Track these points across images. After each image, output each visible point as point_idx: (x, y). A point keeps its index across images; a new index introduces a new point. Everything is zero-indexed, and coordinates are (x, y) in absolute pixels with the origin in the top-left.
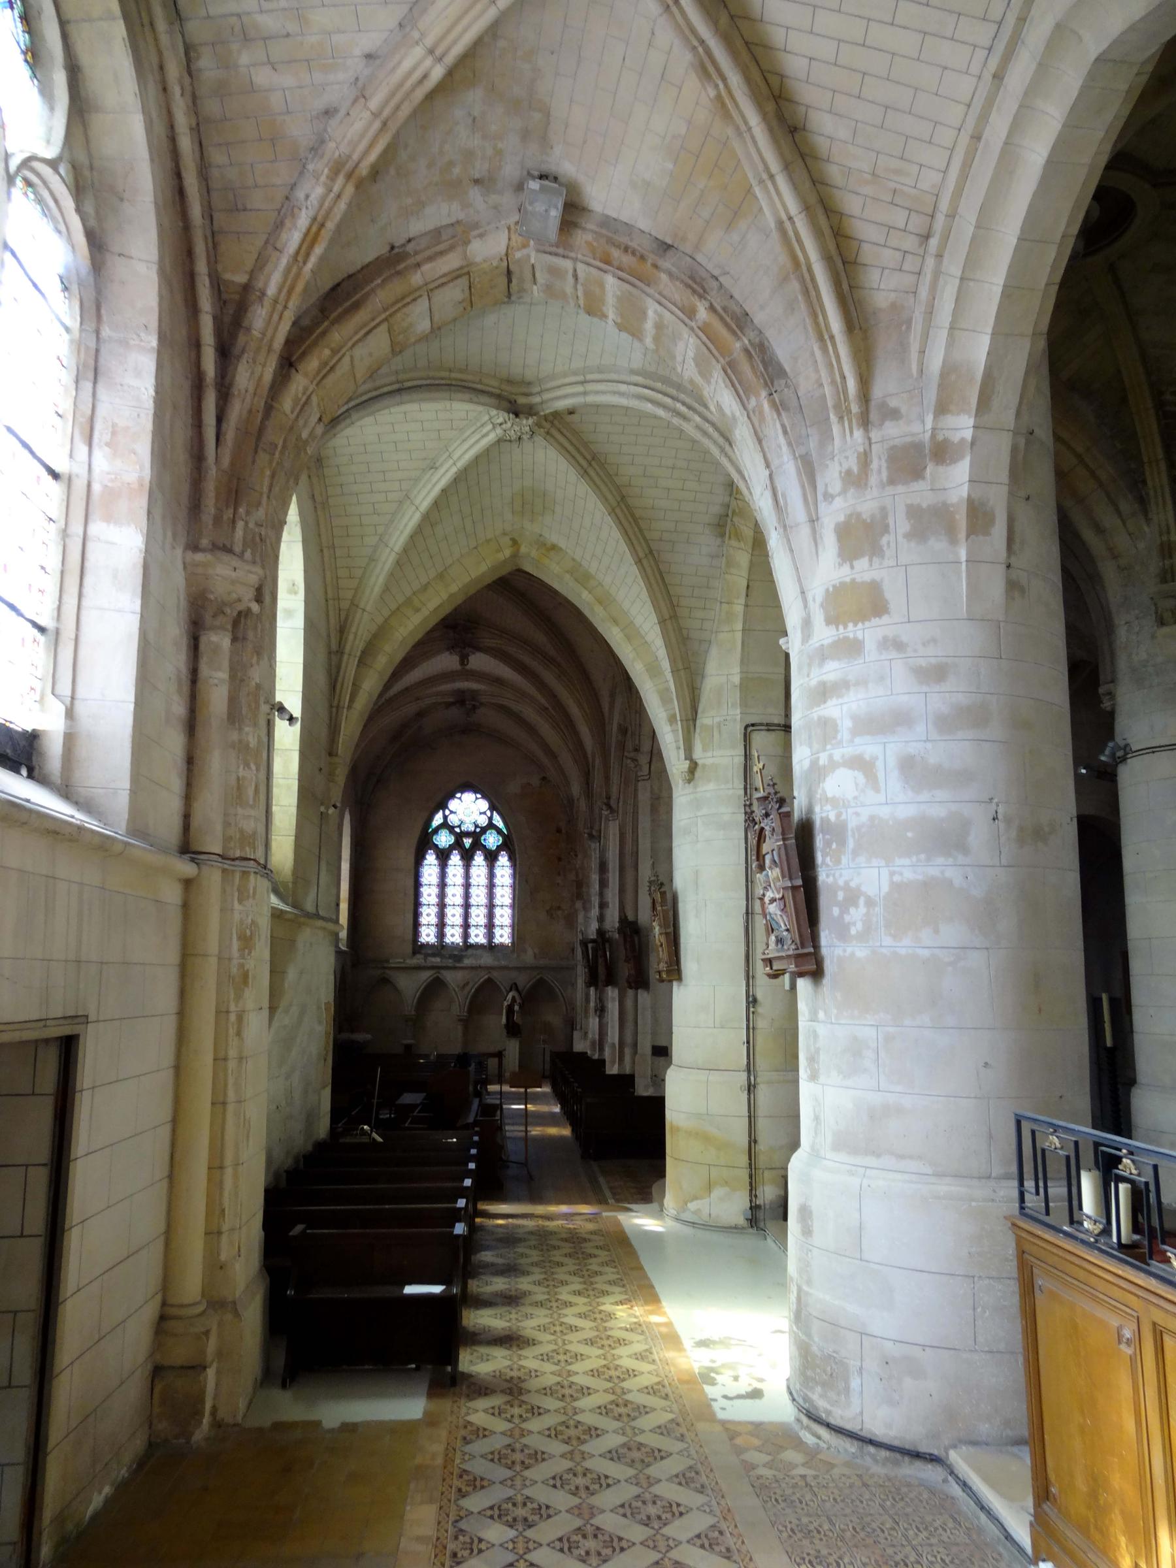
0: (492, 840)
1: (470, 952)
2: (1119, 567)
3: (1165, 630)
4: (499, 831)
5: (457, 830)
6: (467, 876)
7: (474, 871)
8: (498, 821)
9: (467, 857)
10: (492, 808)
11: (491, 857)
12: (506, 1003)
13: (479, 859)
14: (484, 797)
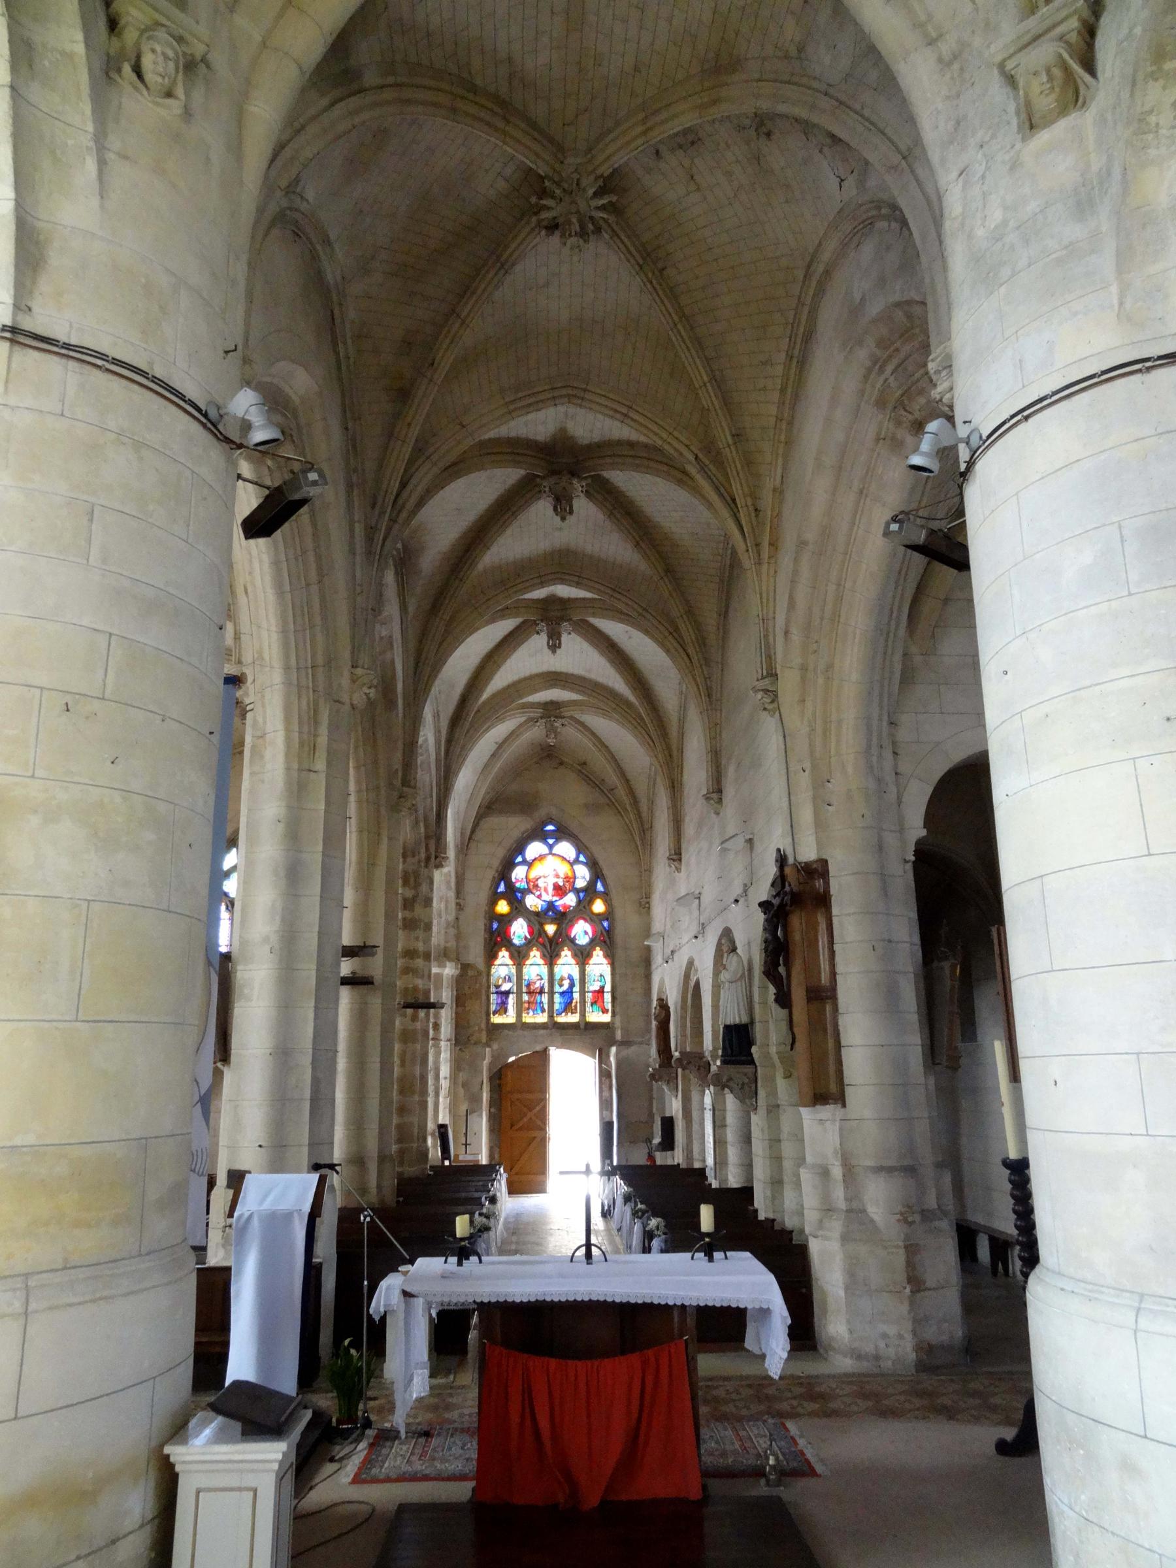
2: (940, 60)
3: (1044, 137)
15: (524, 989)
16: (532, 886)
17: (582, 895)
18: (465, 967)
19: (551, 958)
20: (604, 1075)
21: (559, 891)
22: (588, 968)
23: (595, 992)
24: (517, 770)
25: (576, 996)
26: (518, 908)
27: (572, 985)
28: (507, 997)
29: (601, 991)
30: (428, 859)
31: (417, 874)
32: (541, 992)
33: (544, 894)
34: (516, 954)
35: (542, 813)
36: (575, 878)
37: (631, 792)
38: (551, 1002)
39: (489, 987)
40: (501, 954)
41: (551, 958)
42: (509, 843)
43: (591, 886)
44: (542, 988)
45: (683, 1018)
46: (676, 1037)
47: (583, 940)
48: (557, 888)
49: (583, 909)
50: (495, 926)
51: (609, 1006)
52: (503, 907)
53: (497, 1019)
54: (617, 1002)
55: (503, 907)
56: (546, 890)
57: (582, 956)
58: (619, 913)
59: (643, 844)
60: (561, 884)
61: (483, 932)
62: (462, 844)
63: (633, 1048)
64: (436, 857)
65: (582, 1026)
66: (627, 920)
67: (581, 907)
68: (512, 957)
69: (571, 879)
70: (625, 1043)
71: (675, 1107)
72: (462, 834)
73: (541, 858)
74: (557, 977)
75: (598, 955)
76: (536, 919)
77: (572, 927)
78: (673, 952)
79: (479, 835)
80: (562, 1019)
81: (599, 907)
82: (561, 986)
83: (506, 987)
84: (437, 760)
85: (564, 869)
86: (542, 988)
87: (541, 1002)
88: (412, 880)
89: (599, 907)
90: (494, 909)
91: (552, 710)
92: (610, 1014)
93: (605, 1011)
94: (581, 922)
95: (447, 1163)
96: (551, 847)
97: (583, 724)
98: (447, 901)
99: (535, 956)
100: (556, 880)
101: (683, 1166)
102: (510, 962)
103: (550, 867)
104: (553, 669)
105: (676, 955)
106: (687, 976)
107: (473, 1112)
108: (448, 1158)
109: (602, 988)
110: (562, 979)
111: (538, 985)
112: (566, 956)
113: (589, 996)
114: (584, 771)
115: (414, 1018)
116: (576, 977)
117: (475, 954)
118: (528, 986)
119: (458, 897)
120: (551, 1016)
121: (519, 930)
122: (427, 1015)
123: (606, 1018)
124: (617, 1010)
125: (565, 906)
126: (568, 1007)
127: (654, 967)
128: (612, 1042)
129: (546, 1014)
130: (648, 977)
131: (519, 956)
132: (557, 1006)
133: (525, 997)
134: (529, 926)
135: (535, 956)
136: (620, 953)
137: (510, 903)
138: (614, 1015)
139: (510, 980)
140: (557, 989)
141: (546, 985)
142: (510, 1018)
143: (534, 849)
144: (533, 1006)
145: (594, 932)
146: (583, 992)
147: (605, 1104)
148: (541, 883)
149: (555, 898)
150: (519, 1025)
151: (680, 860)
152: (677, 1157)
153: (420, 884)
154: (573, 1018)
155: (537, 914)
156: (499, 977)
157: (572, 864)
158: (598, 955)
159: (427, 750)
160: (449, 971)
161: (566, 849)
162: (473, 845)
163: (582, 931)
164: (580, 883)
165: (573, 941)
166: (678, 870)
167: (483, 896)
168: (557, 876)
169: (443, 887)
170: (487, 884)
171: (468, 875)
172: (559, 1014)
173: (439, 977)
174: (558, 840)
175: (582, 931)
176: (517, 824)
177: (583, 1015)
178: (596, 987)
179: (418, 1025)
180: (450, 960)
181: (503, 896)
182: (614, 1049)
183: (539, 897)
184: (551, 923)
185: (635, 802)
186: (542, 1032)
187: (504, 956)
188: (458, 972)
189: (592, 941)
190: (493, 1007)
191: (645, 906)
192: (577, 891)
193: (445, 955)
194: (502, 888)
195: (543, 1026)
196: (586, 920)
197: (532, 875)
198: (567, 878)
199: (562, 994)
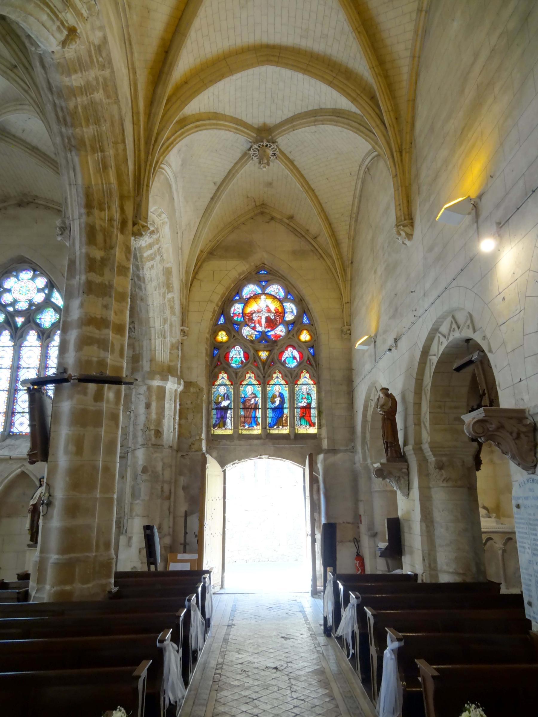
0: (48, 318)
1: (8, 441)
4: (56, 309)
5: (11, 309)
6: (17, 357)
7: (24, 352)
8: (58, 299)
9: (18, 336)
10: (51, 285)
11: (45, 336)
12: (32, 502)
13: (32, 337)
14: (44, 274)
15: (241, 406)
16: (248, 319)
17: (290, 327)
18: (188, 385)
19: (264, 381)
20: (313, 480)
21: (271, 323)
22: (297, 388)
23: (302, 408)
24: (234, 225)
25: (286, 411)
26: (235, 336)
27: (282, 402)
28: (226, 413)
29: (308, 407)
30: (124, 223)
31: (107, 234)
32: (256, 408)
33: (257, 325)
34: (234, 375)
35: (257, 258)
36: (284, 312)
37: (333, 234)
38: (264, 417)
39: (209, 403)
40: (220, 376)
41: (264, 381)
42: (228, 282)
43: (299, 317)
44: (256, 404)
45: (418, 405)
46: (406, 429)
47: (292, 364)
48: (268, 319)
49: (291, 340)
50: (216, 352)
51: (315, 420)
52: (222, 337)
53: (218, 432)
54: (324, 415)
55: (222, 337)
56: (260, 323)
57: (292, 378)
58: (323, 339)
59: (344, 281)
60: (273, 318)
61: (204, 355)
62: (187, 281)
63: (340, 456)
64: (134, 224)
65: (292, 437)
66: (331, 345)
67: (290, 336)
68: (229, 378)
69: (281, 314)
70: (332, 451)
71: (408, 506)
72: (187, 272)
73: (256, 297)
74: (270, 395)
75: (305, 378)
76: (251, 347)
77: (282, 353)
78: (396, 340)
79: (200, 276)
80: (274, 431)
81: (305, 336)
82: (273, 402)
83: (225, 403)
84: (135, 113)
85: (273, 306)
86: (256, 404)
87: (255, 417)
88: (100, 238)
89: (305, 336)
90: (215, 338)
91: (263, 138)
92: (316, 427)
93: (312, 424)
94: (290, 349)
95: (153, 568)
96: (263, 288)
97: (291, 162)
98: (171, 325)
99: (251, 378)
100: (267, 315)
101: (424, 578)
102: (228, 383)
103: (262, 304)
104: (265, 40)
105: (399, 343)
106: (425, 352)
107: (192, 513)
108: (154, 563)
109: (309, 404)
110: (274, 397)
111: (253, 401)
112: (277, 378)
113: (298, 412)
114: (291, 223)
115: (98, 397)
116: (286, 394)
117: (198, 374)
118: (244, 402)
119: (182, 325)
120: (264, 428)
121: (237, 355)
122: (118, 394)
123: (313, 430)
124: (324, 421)
125: (276, 336)
126: (278, 421)
127: (357, 380)
128: (319, 450)
129: (259, 427)
130: (350, 393)
131: (236, 379)
132: (269, 420)
133: (242, 413)
134: (245, 353)
135: (251, 378)
136: (325, 375)
137: (228, 333)
138: (320, 427)
139: (228, 398)
140: (269, 405)
141: (260, 402)
142: (228, 429)
143: (249, 290)
144: (249, 420)
145: (301, 357)
146: (292, 408)
147: (314, 507)
148: (255, 317)
149: (267, 330)
150: (236, 436)
151: (412, 225)
152: (412, 564)
153: (112, 248)
154: (285, 431)
155: (252, 342)
156: (219, 395)
157: (281, 301)
158: (305, 378)
159: (110, 62)
160: (173, 386)
161: (275, 289)
162: (196, 283)
163: (291, 357)
164: (289, 317)
165: (284, 364)
166: (410, 236)
167: (206, 325)
168: (269, 311)
169: (168, 312)
170: (208, 316)
171: (193, 307)
172: (271, 427)
173: (162, 391)
174: (269, 282)
175: (291, 357)
176: (235, 268)
177: (293, 427)
178: (303, 404)
179: (104, 406)
180: (173, 376)
181: (223, 328)
182: (321, 457)
183: (254, 328)
184: (263, 351)
185: (337, 244)
186: (256, 442)
187: (223, 378)
188: (181, 388)
189: (299, 364)
190: (213, 421)
191: (347, 333)
192: (287, 324)
193: (167, 371)
194: (222, 320)
195: (257, 437)
196: (294, 348)
197: (248, 310)
198: (277, 312)
199: (274, 409)
